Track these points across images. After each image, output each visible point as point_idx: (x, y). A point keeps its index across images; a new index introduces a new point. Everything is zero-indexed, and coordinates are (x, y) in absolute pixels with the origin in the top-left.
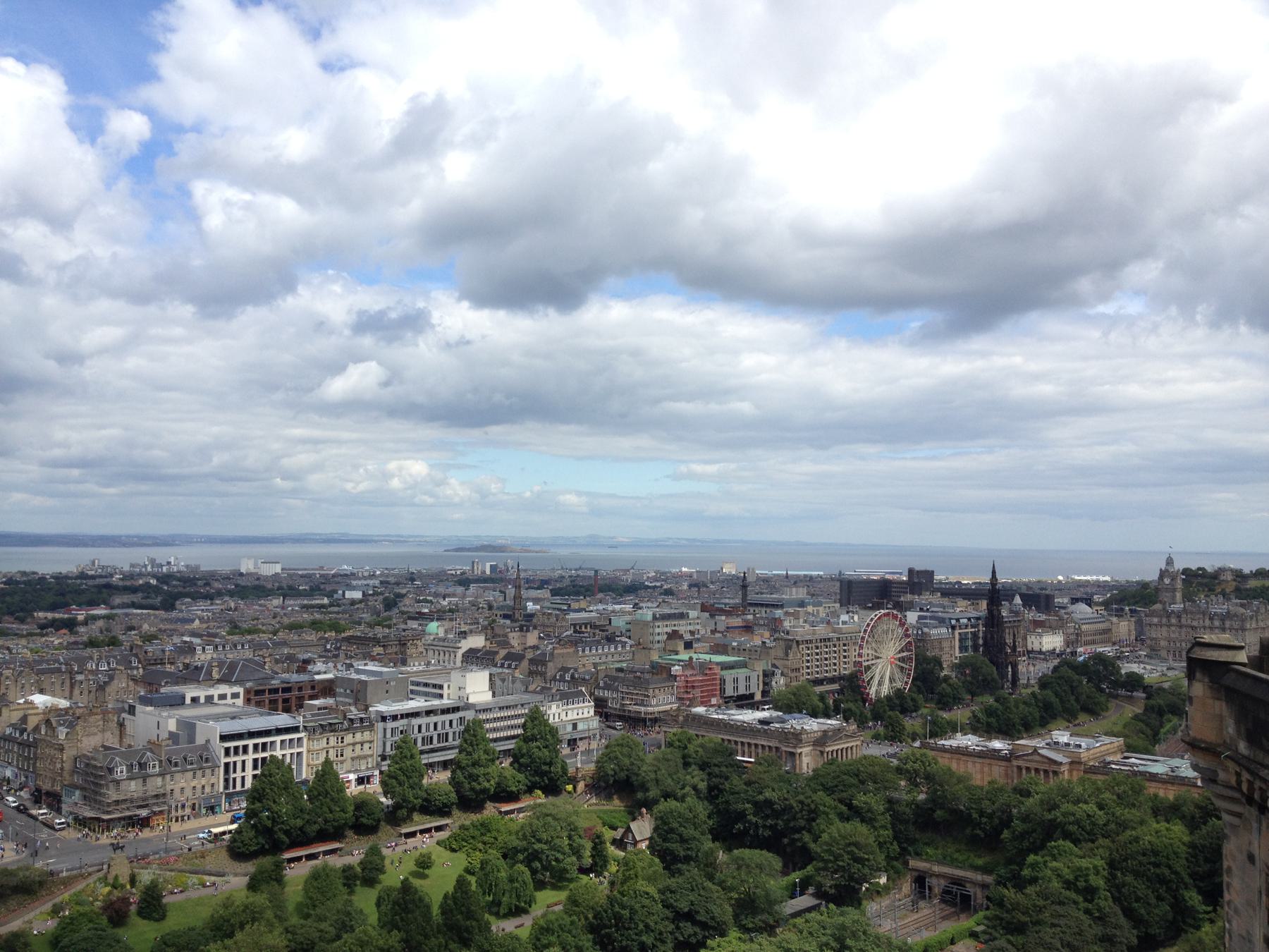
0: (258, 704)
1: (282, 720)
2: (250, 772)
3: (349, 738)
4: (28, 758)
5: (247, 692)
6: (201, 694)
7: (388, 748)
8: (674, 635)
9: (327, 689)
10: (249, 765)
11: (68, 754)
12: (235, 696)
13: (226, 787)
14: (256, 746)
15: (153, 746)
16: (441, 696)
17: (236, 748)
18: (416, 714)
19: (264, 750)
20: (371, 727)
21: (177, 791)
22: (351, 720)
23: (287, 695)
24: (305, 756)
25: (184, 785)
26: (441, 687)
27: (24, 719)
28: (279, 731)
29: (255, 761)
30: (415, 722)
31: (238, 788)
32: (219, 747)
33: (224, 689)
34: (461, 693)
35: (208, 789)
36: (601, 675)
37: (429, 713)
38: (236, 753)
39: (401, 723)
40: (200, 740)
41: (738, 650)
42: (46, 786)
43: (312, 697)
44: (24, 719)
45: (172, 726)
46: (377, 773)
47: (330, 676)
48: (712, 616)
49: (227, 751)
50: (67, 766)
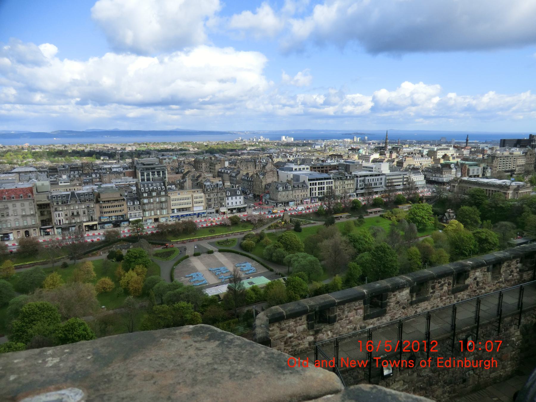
0: (315, 171)
1: (325, 175)
2: (317, 191)
3: (346, 182)
4: (250, 185)
5: (311, 168)
6: (298, 167)
7: (358, 186)
8: (445, 155)
9: (335, 167)
10: (317, 189)
11: (264, 184)
12: (307, 169)
13: (310, 195)
14: (319, 183)
15: (288, 182)
16: (372, 171)
17: (313, 183)
18: (367, 176)
19: (321, 184)
20: (353, 179)
21: (297, 197)
22: (347, 177)
23: (323, 169)
24: (338, 187)
25: (299, 193)
26: (372, 168)
27: (247, 174)
28: (325, 179)
29: (319, 188)
30: (367, 178)
31: (314, 196)
32: (308, 183)
33: (303, 166)
34: (379, 170)
35: (305, 196)
36: (424, 167)
37: (371, 176)
38: (313, 185)
39: (362, 178)
40: (301, 180)
41: (473, 160)
42: (257, 194)
43: (330, 170)
44: (247, 174)
45: (292, 176)
46: (355, 194)
47: (335, 164)
48: (459, 150)
49: (311, 184)
50: (263, 187)
